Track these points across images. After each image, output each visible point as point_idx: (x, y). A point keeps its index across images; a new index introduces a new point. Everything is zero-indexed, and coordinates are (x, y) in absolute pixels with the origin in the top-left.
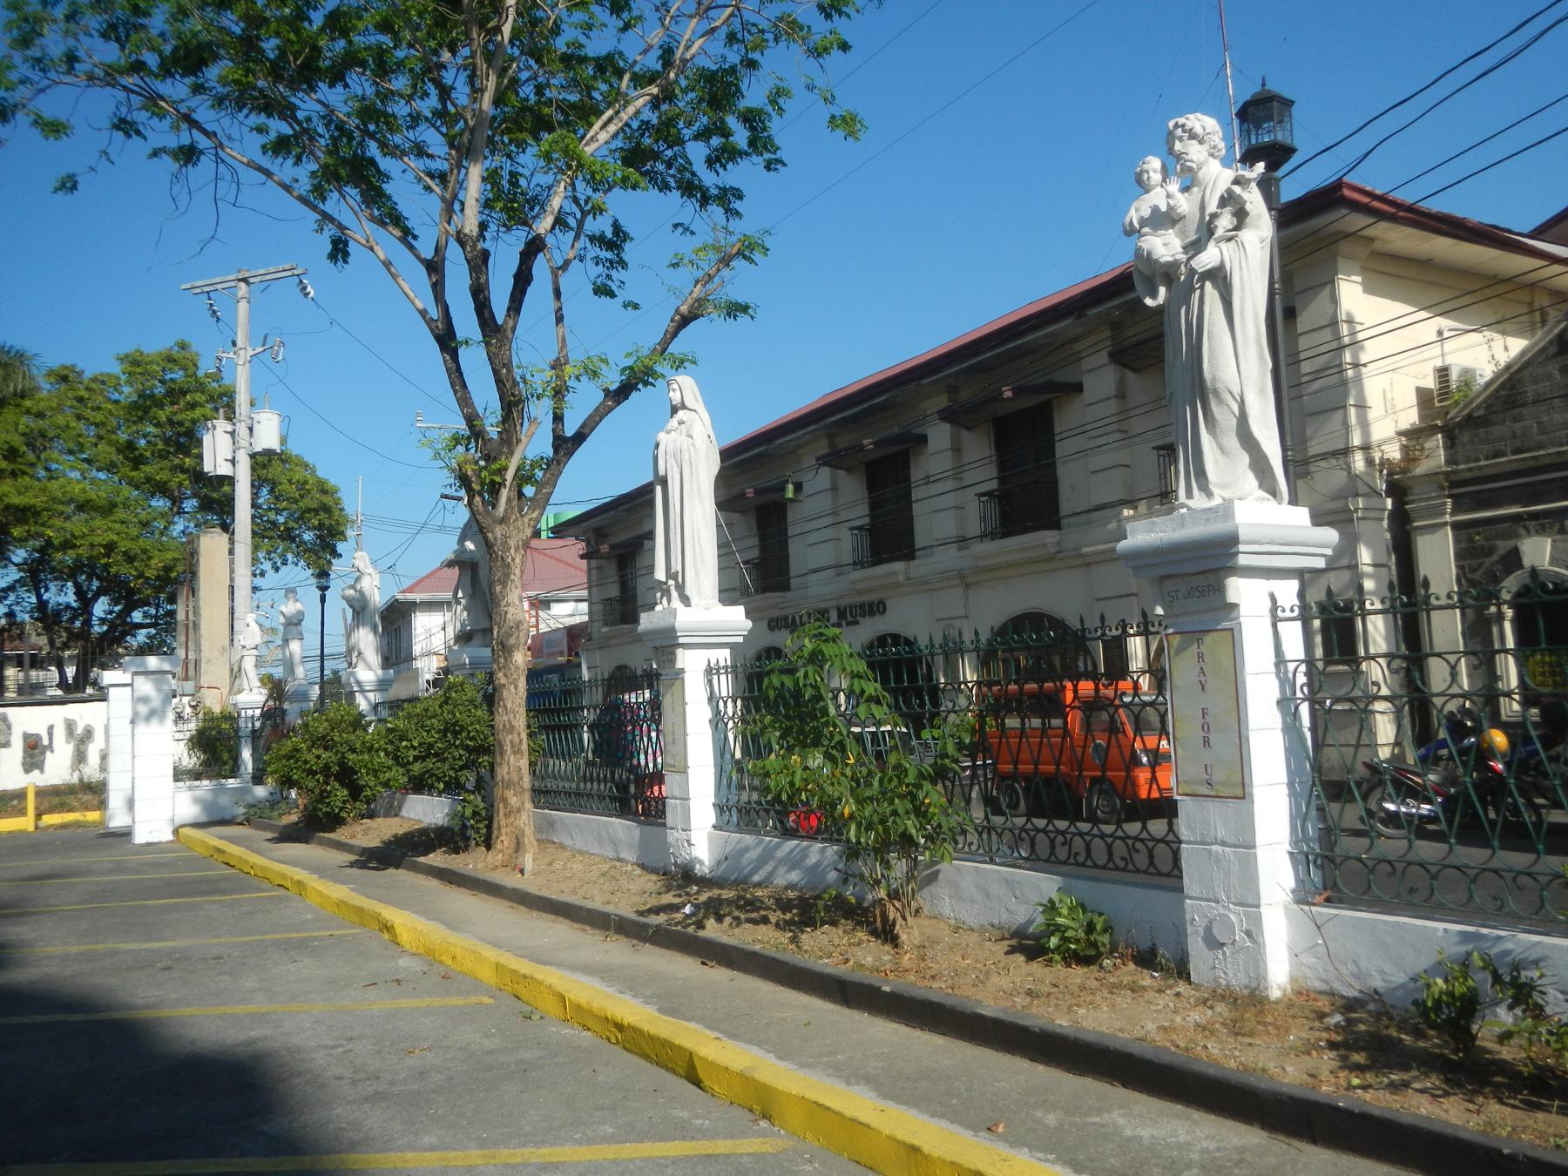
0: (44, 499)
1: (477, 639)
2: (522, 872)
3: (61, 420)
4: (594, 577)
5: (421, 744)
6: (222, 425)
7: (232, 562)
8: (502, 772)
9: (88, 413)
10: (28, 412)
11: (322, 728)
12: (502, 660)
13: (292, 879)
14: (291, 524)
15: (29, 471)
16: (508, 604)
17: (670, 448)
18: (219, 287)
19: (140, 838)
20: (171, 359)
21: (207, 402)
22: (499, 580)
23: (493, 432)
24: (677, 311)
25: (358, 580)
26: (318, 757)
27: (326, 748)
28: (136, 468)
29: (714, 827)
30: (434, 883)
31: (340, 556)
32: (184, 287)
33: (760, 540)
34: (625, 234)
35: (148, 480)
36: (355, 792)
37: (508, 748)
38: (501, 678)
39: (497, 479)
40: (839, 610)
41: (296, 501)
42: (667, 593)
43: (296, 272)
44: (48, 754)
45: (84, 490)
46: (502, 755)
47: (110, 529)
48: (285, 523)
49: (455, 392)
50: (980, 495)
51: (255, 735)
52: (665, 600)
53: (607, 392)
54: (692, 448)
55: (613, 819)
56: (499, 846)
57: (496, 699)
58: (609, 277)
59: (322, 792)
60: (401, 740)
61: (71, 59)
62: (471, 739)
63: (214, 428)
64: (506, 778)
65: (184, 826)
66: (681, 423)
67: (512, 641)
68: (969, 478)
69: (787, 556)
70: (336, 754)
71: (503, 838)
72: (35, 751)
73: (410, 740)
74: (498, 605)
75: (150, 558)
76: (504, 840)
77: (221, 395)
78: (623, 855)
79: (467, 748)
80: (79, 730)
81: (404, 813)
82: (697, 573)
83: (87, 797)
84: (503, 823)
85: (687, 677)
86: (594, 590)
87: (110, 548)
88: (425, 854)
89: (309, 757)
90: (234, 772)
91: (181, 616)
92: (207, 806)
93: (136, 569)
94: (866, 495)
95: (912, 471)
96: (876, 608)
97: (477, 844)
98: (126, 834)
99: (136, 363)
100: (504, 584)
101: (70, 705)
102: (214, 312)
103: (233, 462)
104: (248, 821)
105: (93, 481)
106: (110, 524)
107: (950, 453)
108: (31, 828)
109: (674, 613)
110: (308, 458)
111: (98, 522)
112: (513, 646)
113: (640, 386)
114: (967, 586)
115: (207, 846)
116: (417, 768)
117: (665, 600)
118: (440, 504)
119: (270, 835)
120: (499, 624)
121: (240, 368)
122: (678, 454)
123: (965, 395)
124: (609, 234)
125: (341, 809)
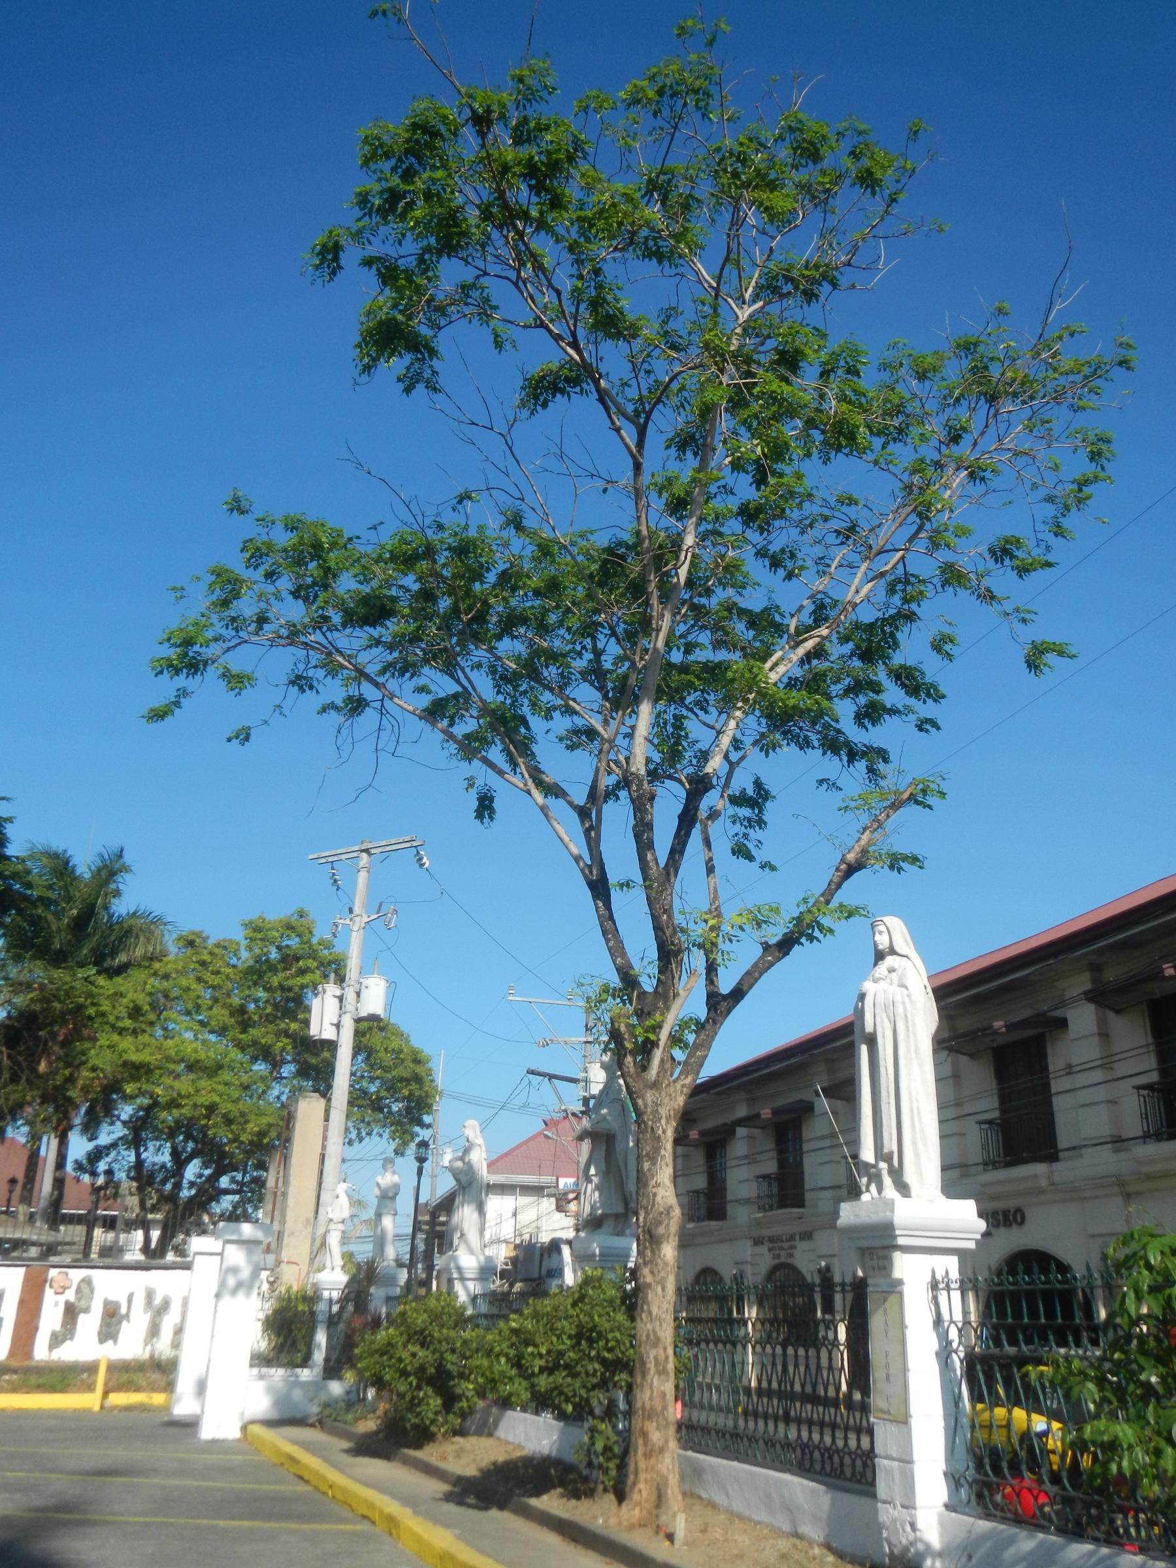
0: (159, 1057)
1: (608, 1226)
2: (670, 1537)
3: (184, 982)
4: (680, 1167)
5: (549, 1352)
6: (332, 989)
7: (326, 1129)
8: (643, 1397)
9: (208, 977)
10: (155, 974)
11: (421, 1320)
12: (648, 1252)
13: (381, 1511)
14: (383, 1094)
15: (148, 1029)
16: (657, 1185)
17: (880, 1000)
18: (343, 857)
19: (207, 1432)
20: (290, 927)
21: (318, 968)
22: (647, 1155)
23: (648, 985)
24: (843, 860)
25: (467, 1151)
26: (414, 1355)
27: (422, 1345)
28: (244, 1031)
29: (947, 1507)
30: (552, 1539)
32: (311, 857)
34: (767, 792)
35: (255, 1043)
36: (450, 1400)
37: (651, 1366)
38: (646, 1275)
39: (652, 1037)
41: (387, 1070)
42: (876, 1178)
43: (414, 844)
44: (124, 1323)
45: (196, 1050)
46: (644, 1375)
47: (213, 1090)
48: (378, 1092)
49: (607, 941)
50: (1138, 1088)
51: (332, 1322)
52: (873, 1188)
53: (766, 947)
54: (907, 1000)
55: (787, 1477)
56: (636, 1497)
57: (640, 1302)
58: (746, 836)
59: (413, 1398)
60: (527, 1343)
61: (262, 620)
62: (610, 1350)
64: (648, 1407)
65: (252, 1422)
66: (891, 970)
67: (661, 1230)
68: (1122, 1069)
70: (434, 1352)
71: (641, 1485)
72: (112, 1318)
73: (536, 1345)
74: (646, 1185)
75: (246, 1122)
76: (642, 1491)
77: (330, 963)
78: (805, 1529)
79: (603, 1361)
80: (157, 1301)
81: (501, 1432)
82: (917, 1155)
83: (155, 1376)
84: (642, 1465)
85: (907, 1290)
86: (679, 1180)
87: (211, 1109)
88: (538, 1493)
89: (405, 1355)
90: (305, 1362)
91: (270, 1183)
92: (281, 1401)
93: (232, 1132)
94: (994, 1085)
95: (1050, 1059)
97: (605, 1490)
98: (190, 1425)
99: (258, 929)
100: (653, 1161)
101: (153, 1272)
102: (335, 881)
103: (338, 1026)
104: (320, 1423)
105: (204, 1042)
106: (215, 1086)
107: (1096, 1039)
108: (97, 1408)
109: (891, 1204)
110: (404, 1028)
111: (204, 1083)
112: (663, 1236)
113: (803, 940)
114: (1128, 1197)
115: (278, 1452)
116: (543, 1382)
117: (873, 1188)
118: (526, 1081)
119: (346, 1445)
120: (646, 1208)
121: (354, 934)
122: (890, 1007)
123: (1112, 974)
124: (750, 792)
125: (433, 1422)
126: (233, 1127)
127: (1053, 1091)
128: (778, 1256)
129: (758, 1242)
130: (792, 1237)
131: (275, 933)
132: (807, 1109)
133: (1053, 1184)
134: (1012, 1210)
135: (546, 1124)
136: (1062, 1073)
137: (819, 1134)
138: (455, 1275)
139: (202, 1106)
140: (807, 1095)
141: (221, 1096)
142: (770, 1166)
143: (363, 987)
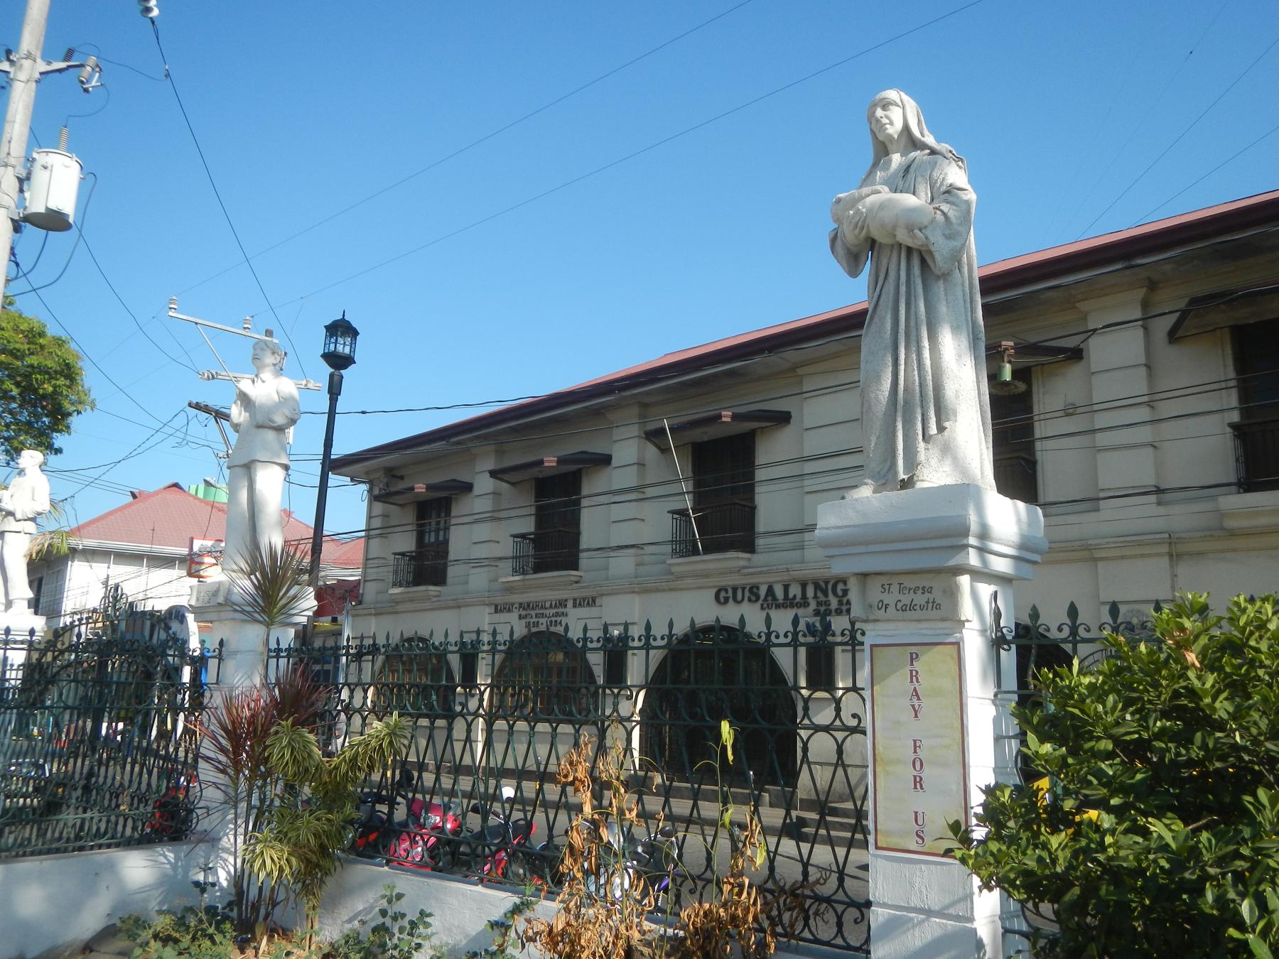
31: (58, 451)
33: (695, 487)
69: (753, 508)
86: (375, 543)
114: (1175, 557)
127: (1037, 435)
130: (562, 604)
132: (605, 460)
135: (134, 496)
136: (1061, 413)
137: (614, 487)
140: (597, 446)
142: (528, 525)
143: (37, 167)
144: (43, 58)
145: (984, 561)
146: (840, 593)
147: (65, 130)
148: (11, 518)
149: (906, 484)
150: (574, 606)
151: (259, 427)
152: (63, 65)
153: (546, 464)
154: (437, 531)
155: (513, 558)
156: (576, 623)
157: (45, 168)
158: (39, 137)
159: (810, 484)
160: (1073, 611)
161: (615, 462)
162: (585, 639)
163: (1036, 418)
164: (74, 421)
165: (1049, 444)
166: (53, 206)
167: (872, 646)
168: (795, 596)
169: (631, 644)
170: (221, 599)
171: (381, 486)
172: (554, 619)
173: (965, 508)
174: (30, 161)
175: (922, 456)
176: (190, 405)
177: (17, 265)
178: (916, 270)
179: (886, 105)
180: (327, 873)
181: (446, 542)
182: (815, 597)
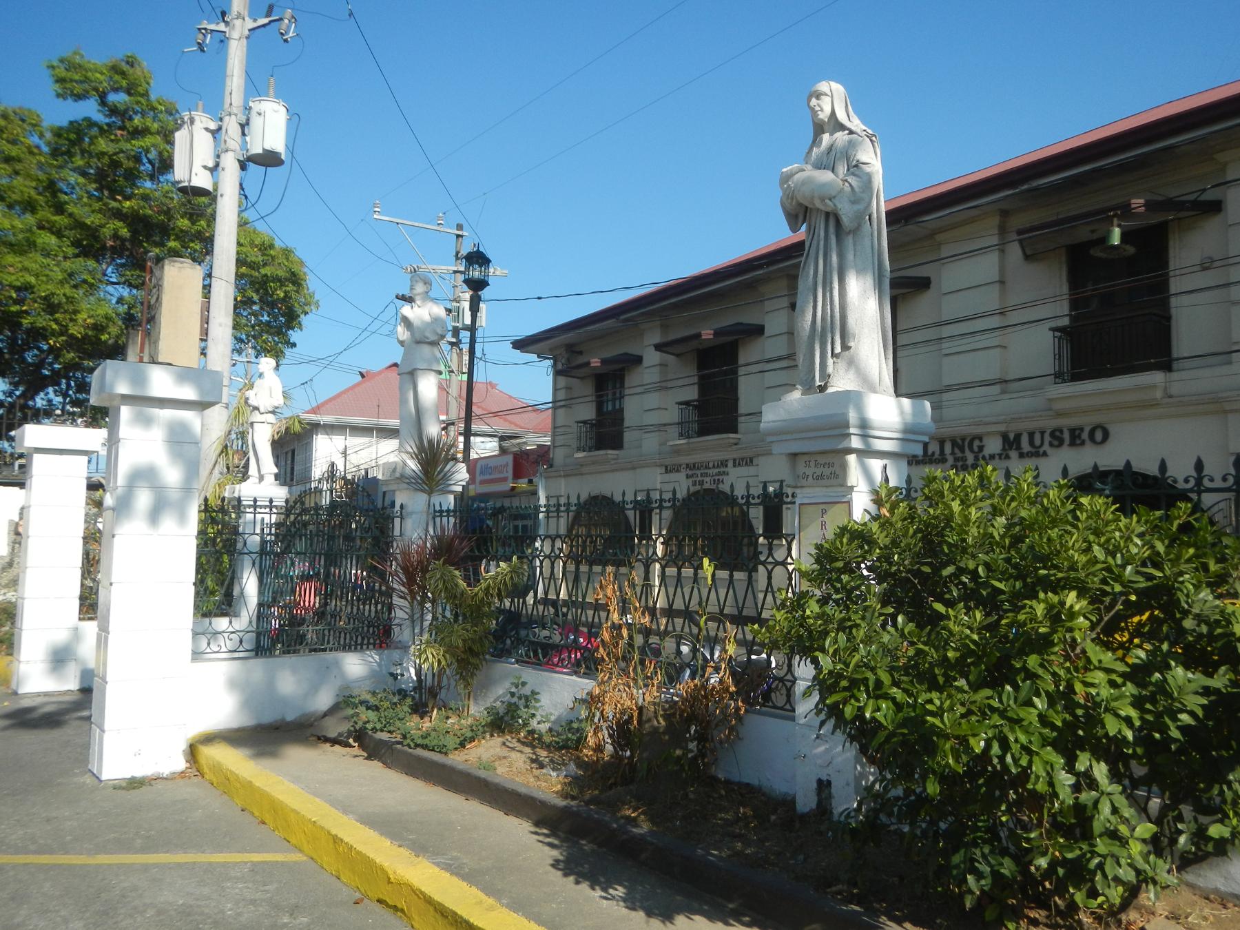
7: (206, 308)
21: (158, 133)
31: (294, 345)
40: (1005, 436)
47: (25, 269)
63: (192, 121)
65: (209, 739)
75: (76, 312)
86: (561, 412)
93: (56, 321)
94: (1065, 289)
96: (1100, 434)
103: (214, 169)
126: (57, 315)
127: (1173, 290)
128: (701, 483)
129: (668, 470)
130: (724, 464)
131: (98, 75)
132: (759, 330)
133: (1171, 397)
134: (1087, 430)
136: (1198, 268)
137: (768, 357)
138: (856, 443)
139: (12, 286)
140: (749, 317)
141: (37, 276)
142: (692, 394)
143: (254, 113)
144: (250, 16)
145: (867, 444)
146: (976, 449)
147: (272, 80)
148: (257, 412)
149: (822, 389)
150: (734, 466)
151: (418, 342)
152: (266, 21)
153: (704, 337)
154: (614, 400)
155: (678, 424)
156: (737, 482)
157: (260, 114)
158: (254, 88)
159: (948, 347)
160: (1199, 466)
161: (767, 332)
162: (624, 501)
163: (1171, 274)
164: (304, 319)
165: (1185, 300)
166: (268, 147)
167: (801, 504)
168: (933, 453)
169: (785, 499)
170: (397, 475)
171: (563, 361)
172: (717, 478)
173: (847, 407)
174: (248, 109)
175: (830, 369)
176: (397, 297)
177: (246, 197)
178: (832, 229)
179: (818, 96)
180: (476, 667)
181: (621, 410)
182: (953, 453)
